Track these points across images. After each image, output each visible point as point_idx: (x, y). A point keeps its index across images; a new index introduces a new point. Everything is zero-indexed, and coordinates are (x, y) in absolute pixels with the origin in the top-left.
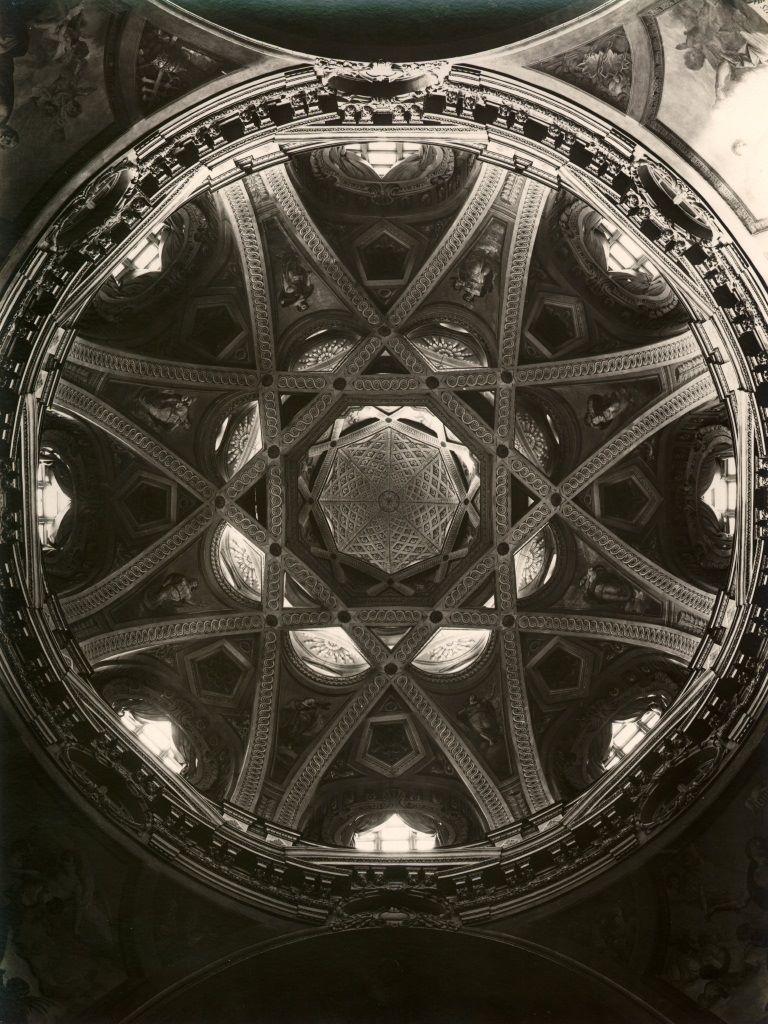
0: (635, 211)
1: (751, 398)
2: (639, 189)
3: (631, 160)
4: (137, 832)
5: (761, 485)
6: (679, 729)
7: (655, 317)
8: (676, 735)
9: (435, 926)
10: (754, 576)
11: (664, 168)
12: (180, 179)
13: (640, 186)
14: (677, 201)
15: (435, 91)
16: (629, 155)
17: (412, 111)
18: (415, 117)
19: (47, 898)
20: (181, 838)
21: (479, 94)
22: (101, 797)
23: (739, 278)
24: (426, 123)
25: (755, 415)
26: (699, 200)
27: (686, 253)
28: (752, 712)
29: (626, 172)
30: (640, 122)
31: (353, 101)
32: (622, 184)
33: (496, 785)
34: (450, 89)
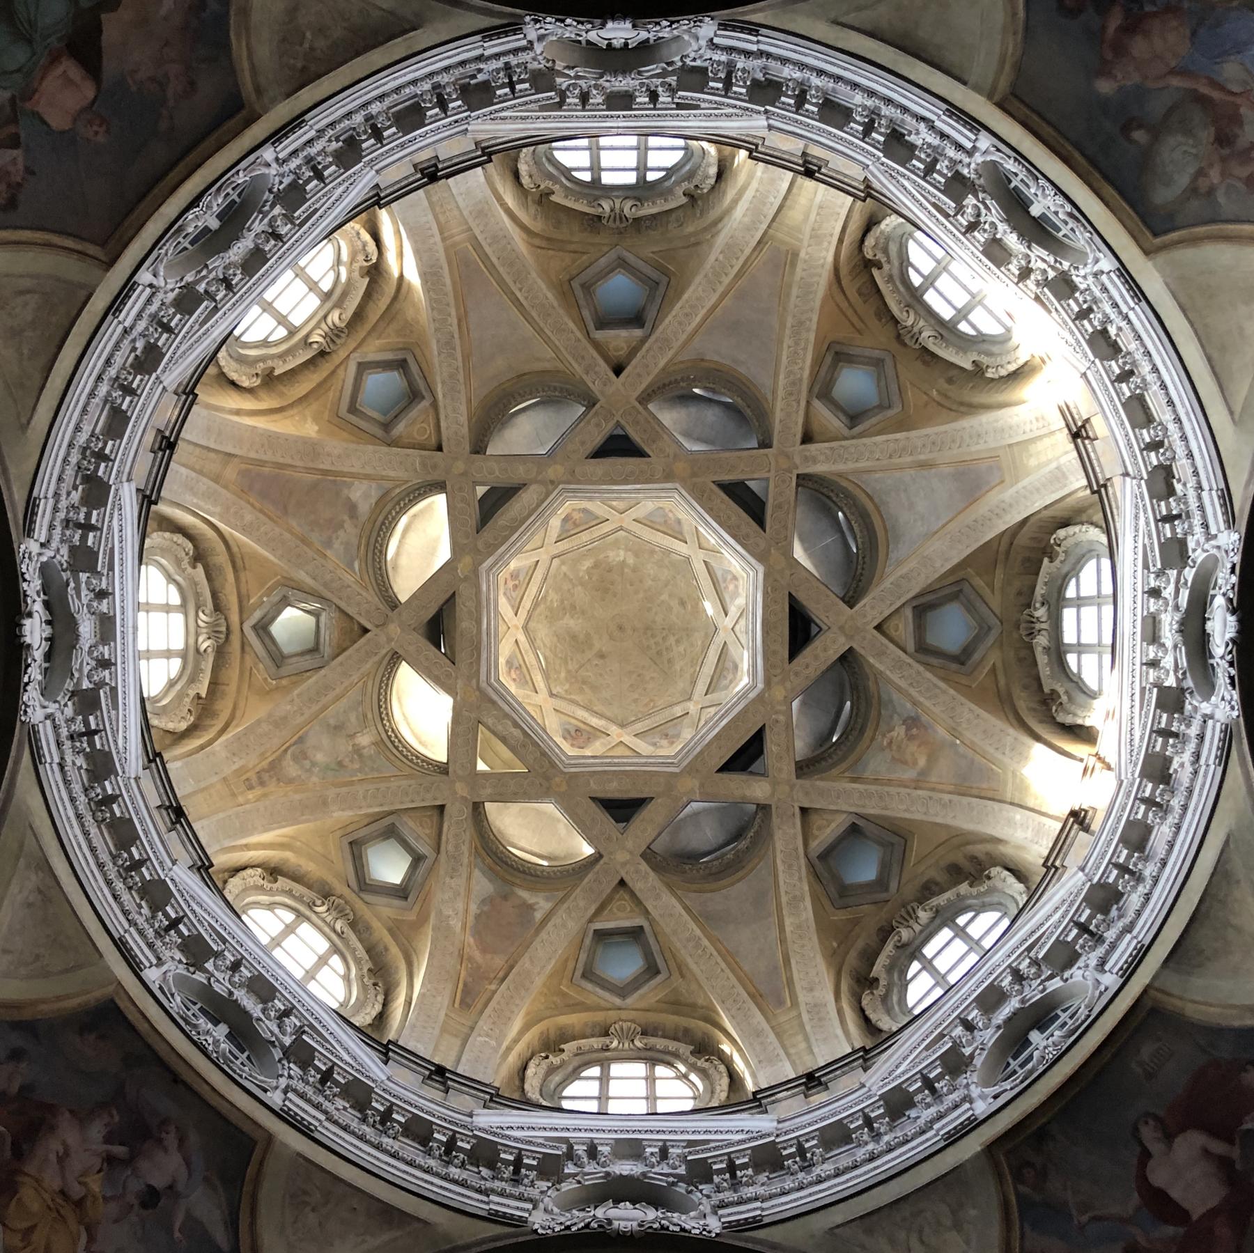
0: (972, 227)
1: (1139, 486)
2: (981, 195)
3: (970, 153)
4: (266, 1091)
5: (1152, 610)
6: (1032, 954)
7: (996, 376)
8: (1028, 961)
9: (683, 1230)
10: (1142, 739)
11: (1020, 163)
13: (984, 192)
14: (1035, 211)
15: (694, 60)
16: (969, 145)
17: (660, 89)
18: (664, 98)
19: (135, 1186)
20: (326, 1097)
21: (759, 62)
22: (216, 1042)
23: (1126, 317)
24: (679, 106)
25: (1145, 512)
26: (1068, 208)
27: (1046, 283)
28: (1139, 933)
29: (965, 171)
30: (990, 97)
31: (577, 77)
32: (958, 186)
33: (768, 1020)
34: (716, 57)
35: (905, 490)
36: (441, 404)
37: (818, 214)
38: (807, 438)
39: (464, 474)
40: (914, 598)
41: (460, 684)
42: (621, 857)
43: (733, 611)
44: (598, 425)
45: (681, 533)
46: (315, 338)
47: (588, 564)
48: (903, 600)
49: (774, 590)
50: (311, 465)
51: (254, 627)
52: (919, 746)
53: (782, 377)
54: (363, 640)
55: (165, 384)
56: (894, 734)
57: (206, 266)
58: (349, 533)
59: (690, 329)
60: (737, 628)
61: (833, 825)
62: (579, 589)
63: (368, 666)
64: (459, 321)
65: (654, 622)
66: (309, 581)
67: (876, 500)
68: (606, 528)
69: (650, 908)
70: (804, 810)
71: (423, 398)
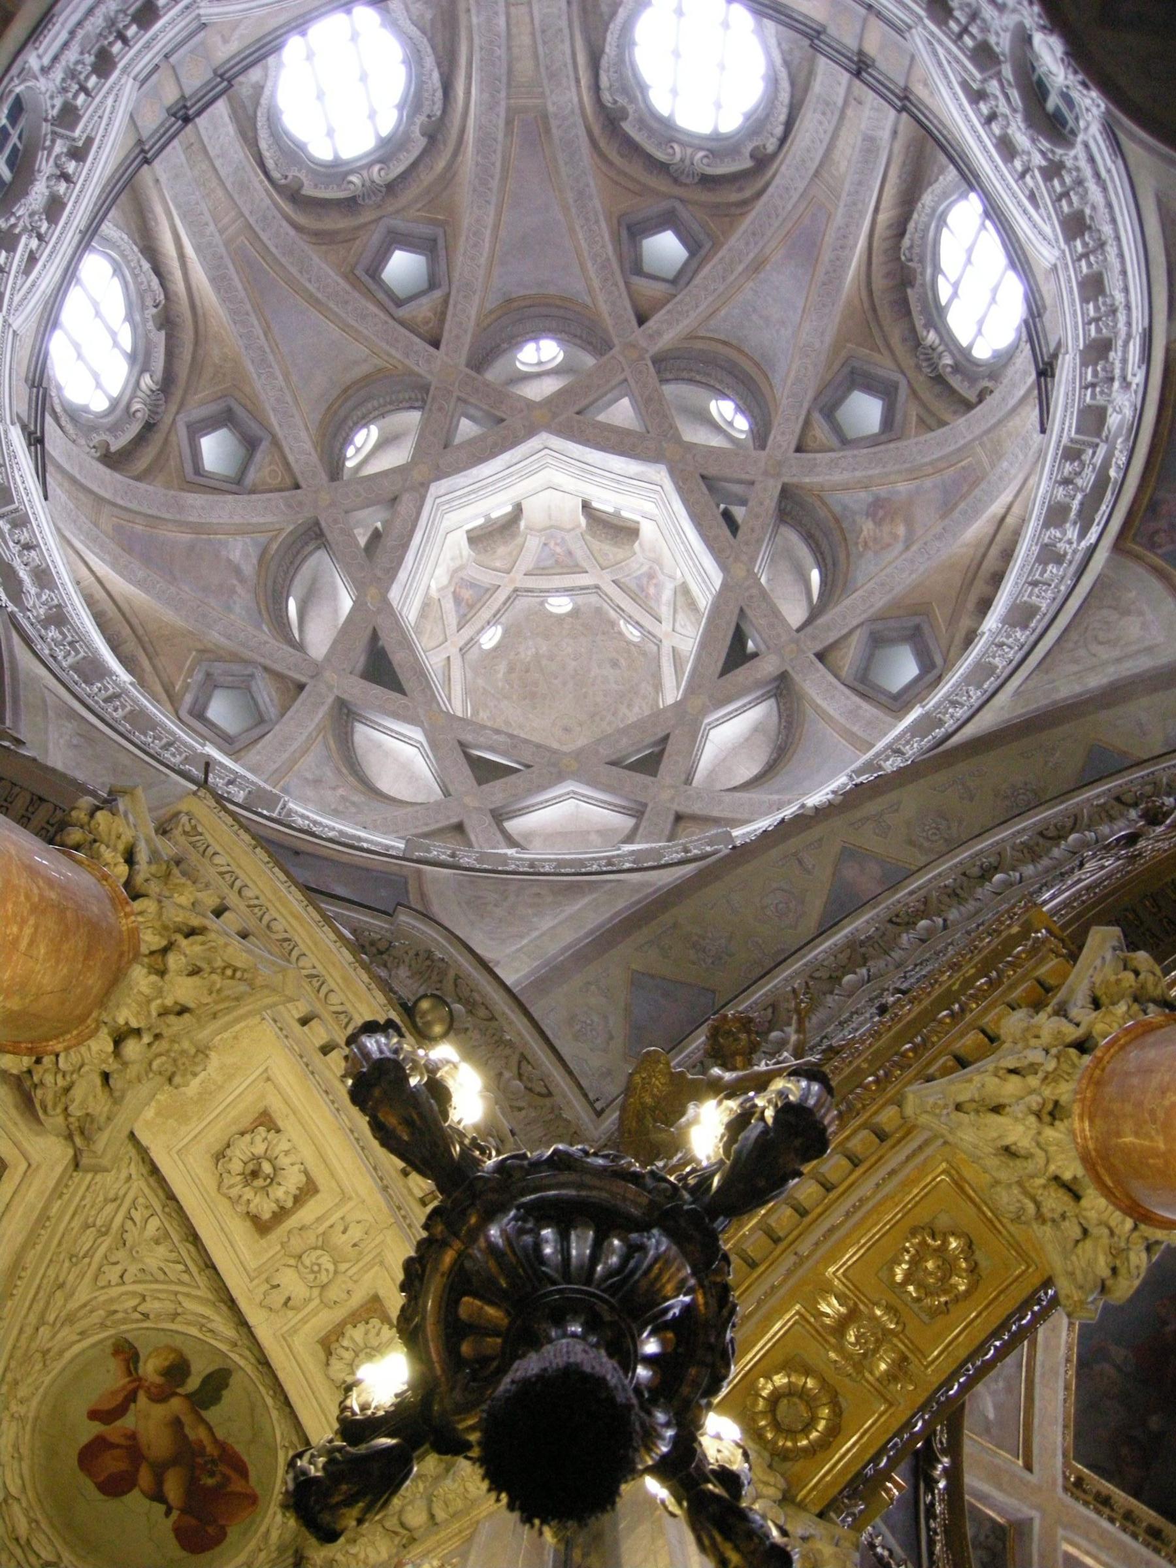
12: (105, 97)
35: (755, 310)
36: (280, 434)
37: (545, 43)
38: (642, 320)
39: (333, 504)
40: (815, 399)
41: (421, 711)
42: (666, 795)
43: (665, 611)
44: (440, 409)
45: (577, 565)
46: (136, 406)
47: (502, 668)
48: (806, 405)
49: (685, 481)
50: (178, 517)
51: (191, 713)
52: (892, 520)
53: (589, 265)
54: (304, 694)
55: (15, 326)
56: (865, 532)
57: (13, 214)
58: (243, 599)
59: (483, 261)
60: (678, 628)
61: (854, 643)
62: (505, 703)
63: (320, 715)
64: (266, 335)
65: (596, 704)
66: (223, 641)
67: (734, 342)
68: (501, 596)
69: (716, 813)
70: (821, 656)
71: (260, 440)
